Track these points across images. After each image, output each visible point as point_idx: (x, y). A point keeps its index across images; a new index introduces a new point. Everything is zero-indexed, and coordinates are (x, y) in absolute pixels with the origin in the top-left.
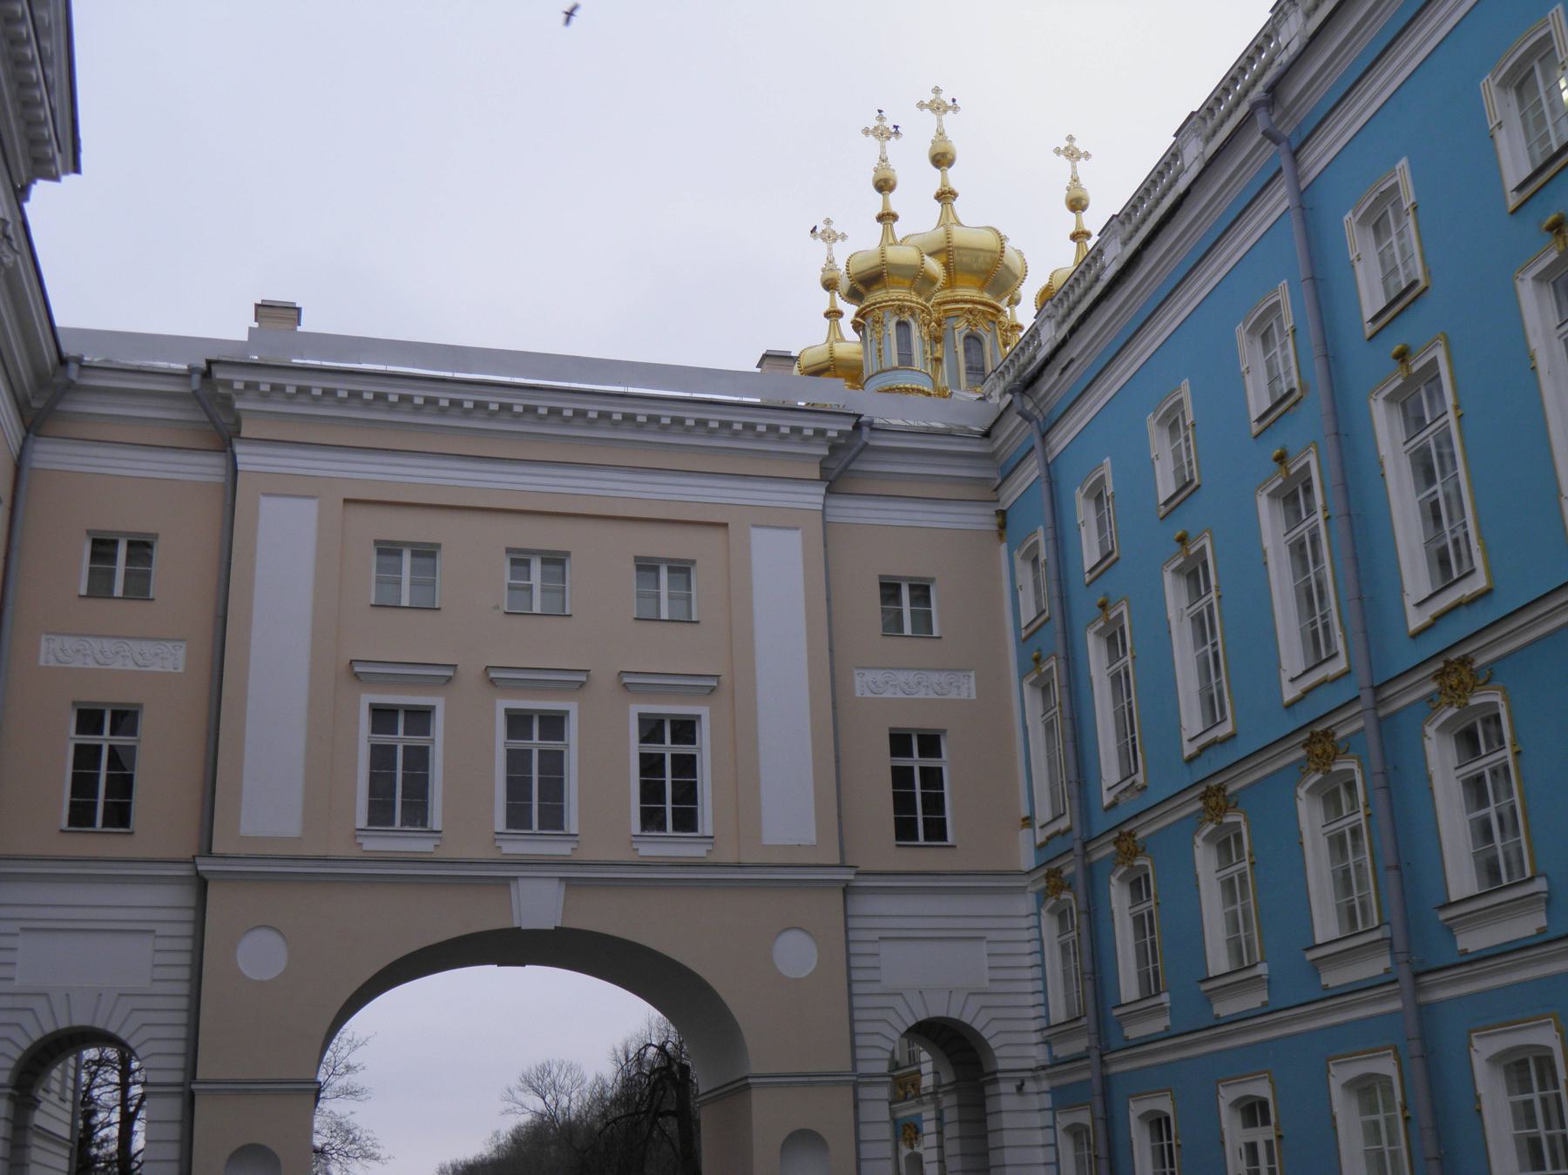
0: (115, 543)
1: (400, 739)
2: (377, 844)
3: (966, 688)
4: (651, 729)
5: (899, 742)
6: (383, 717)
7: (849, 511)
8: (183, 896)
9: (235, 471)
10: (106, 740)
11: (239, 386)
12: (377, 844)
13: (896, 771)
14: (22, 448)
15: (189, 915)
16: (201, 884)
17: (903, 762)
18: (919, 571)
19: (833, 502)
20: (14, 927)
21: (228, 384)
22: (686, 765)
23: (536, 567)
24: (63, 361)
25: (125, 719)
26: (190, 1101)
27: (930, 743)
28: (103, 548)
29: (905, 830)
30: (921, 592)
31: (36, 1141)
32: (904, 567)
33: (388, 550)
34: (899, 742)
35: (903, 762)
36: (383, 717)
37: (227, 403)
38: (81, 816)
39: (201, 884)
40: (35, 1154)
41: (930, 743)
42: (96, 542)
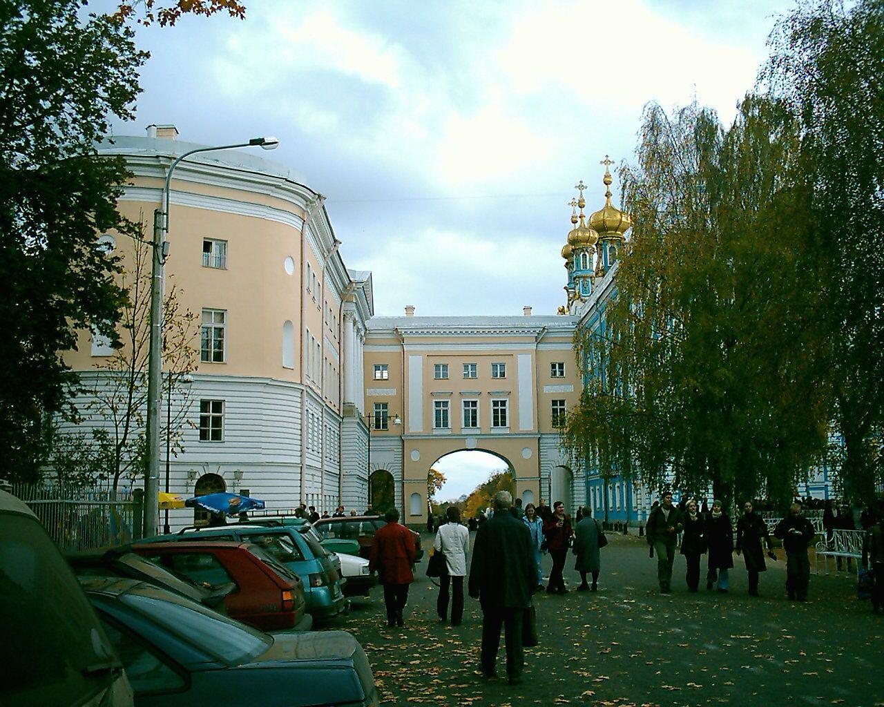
2: (435, 433)
3: (571, 389)
4: (495, 403)
5: (554, 403)
7: (542, 347)
13: (553, 409)
17: (555, 407)
18: (561, 362)
19: (539, 345)
22: (503, 411)
25: (385, 406)
26: (403, 484)
27: (562, 403)
29: (554, 423)
30: (561, 366)
32: (557, 361)
33: (437, 366)
34: (554, 403)
35: (555, 407)
36: (438, 404)
41: (562, 403)
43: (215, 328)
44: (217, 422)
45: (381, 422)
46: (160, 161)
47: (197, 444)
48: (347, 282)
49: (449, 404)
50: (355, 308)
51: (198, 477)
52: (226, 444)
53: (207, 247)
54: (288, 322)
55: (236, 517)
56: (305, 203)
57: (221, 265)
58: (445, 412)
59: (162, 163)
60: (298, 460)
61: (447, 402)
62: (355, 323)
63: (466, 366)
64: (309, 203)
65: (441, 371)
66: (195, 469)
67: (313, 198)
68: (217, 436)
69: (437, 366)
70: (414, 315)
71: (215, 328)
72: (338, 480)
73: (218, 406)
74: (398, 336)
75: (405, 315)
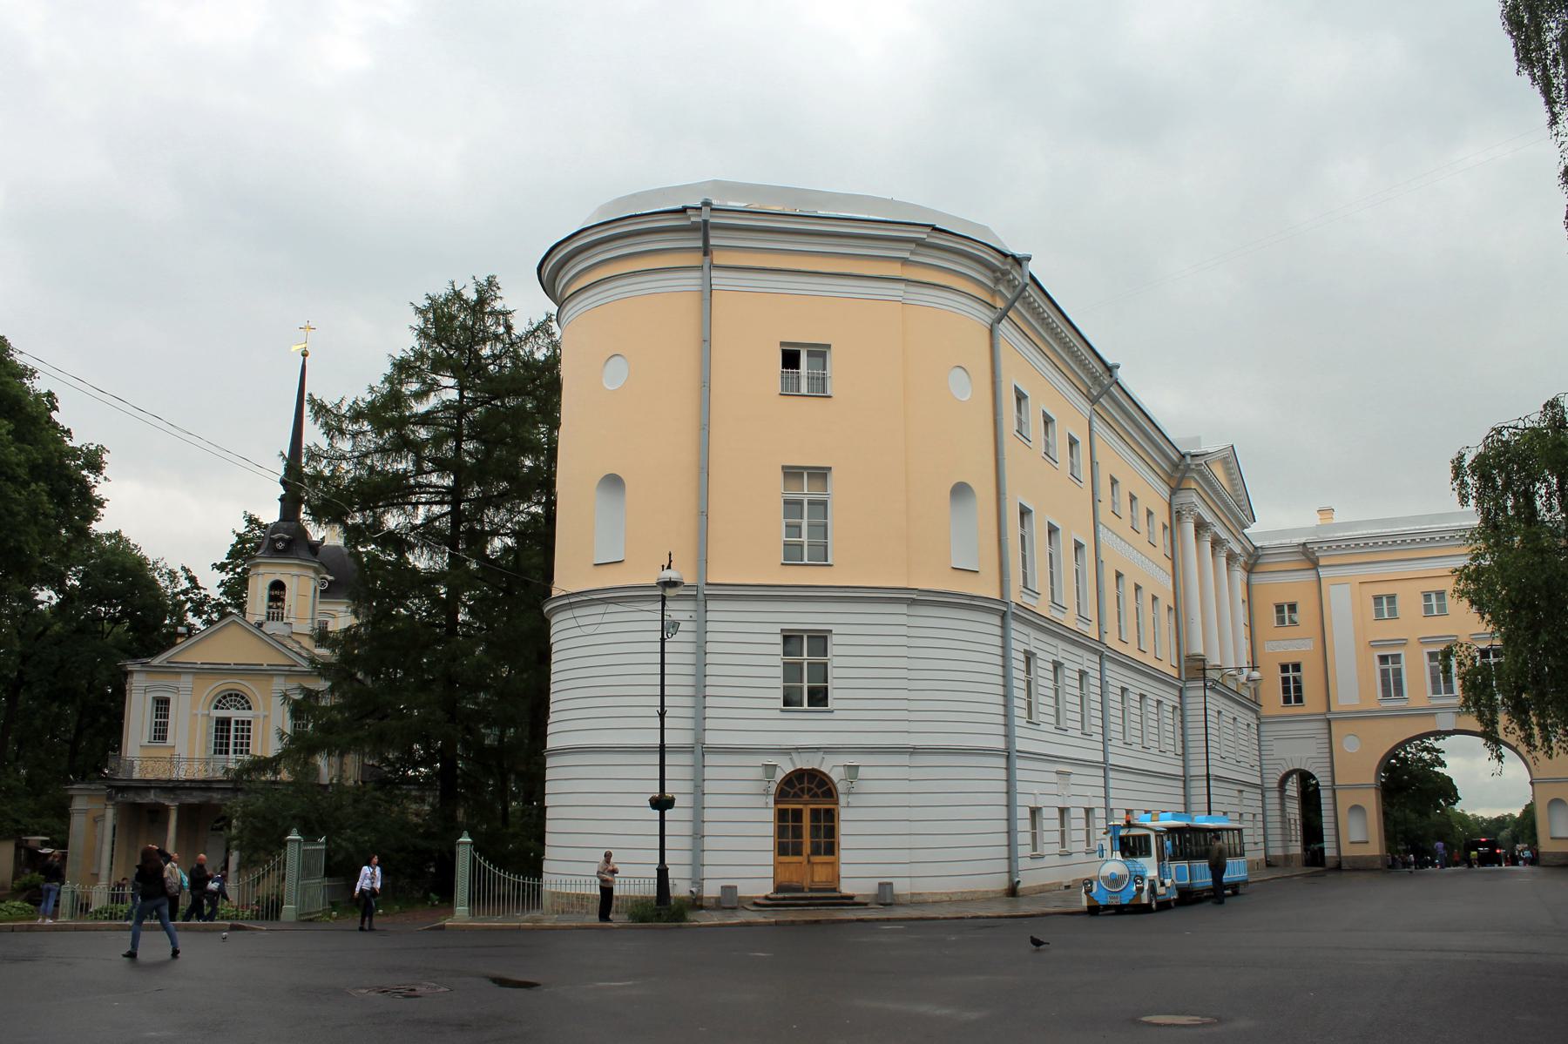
0: (1283, 606)
1: (1390, 666)
2: (1385, 704)
6: (1383, 659)
8: (1324, 725)
9: (1320, 579)
10: (1291, 674)
11: (1316, 549)
12: (1385, 704)
14: (1248, 579)
15: (1326, 731)
16: (1329, 721)
20: (1271, 738)
21: (1312, 548)
23: (1433, 597)
24: (1256, 548)
25: (1297, 667)
28: (1280, 608)
31: (1287, 800)
36: (1383, 659)
37: (1313, 553)
38: (1287, 700)
39: (1329, 721)
40: (1288, 804)
42: (1277, 607)
43: (810, 503)
44: (821, 671)
45: (1293, 692)
46: (689, 218)
47: (778, 714)
48: (1175, 457)
49: (1403, 657)
50: (1195, 499)
51: (780, 776)
52: (837, 715)
53: (790, 359)
54: (961, 491)
55: (322, 844)
56: (989, 274)
57: (819, 388)
58: (1398, 672)
59: (693, 219)
60: (1000, 743)
61: (1399, 655)
62: (1201, 526)
63: (1427, 596)
64: (999, 274)
65: (1385, 604)
66: (772, 760)
67: (1004, 264)
68: (819, 697)
69: (1378, 599)
70: (1334, 522)
71: (810, 503)
72: (1181, 791)
73: (820, 640)
74: (1309, 556)
75: (1319, 523)
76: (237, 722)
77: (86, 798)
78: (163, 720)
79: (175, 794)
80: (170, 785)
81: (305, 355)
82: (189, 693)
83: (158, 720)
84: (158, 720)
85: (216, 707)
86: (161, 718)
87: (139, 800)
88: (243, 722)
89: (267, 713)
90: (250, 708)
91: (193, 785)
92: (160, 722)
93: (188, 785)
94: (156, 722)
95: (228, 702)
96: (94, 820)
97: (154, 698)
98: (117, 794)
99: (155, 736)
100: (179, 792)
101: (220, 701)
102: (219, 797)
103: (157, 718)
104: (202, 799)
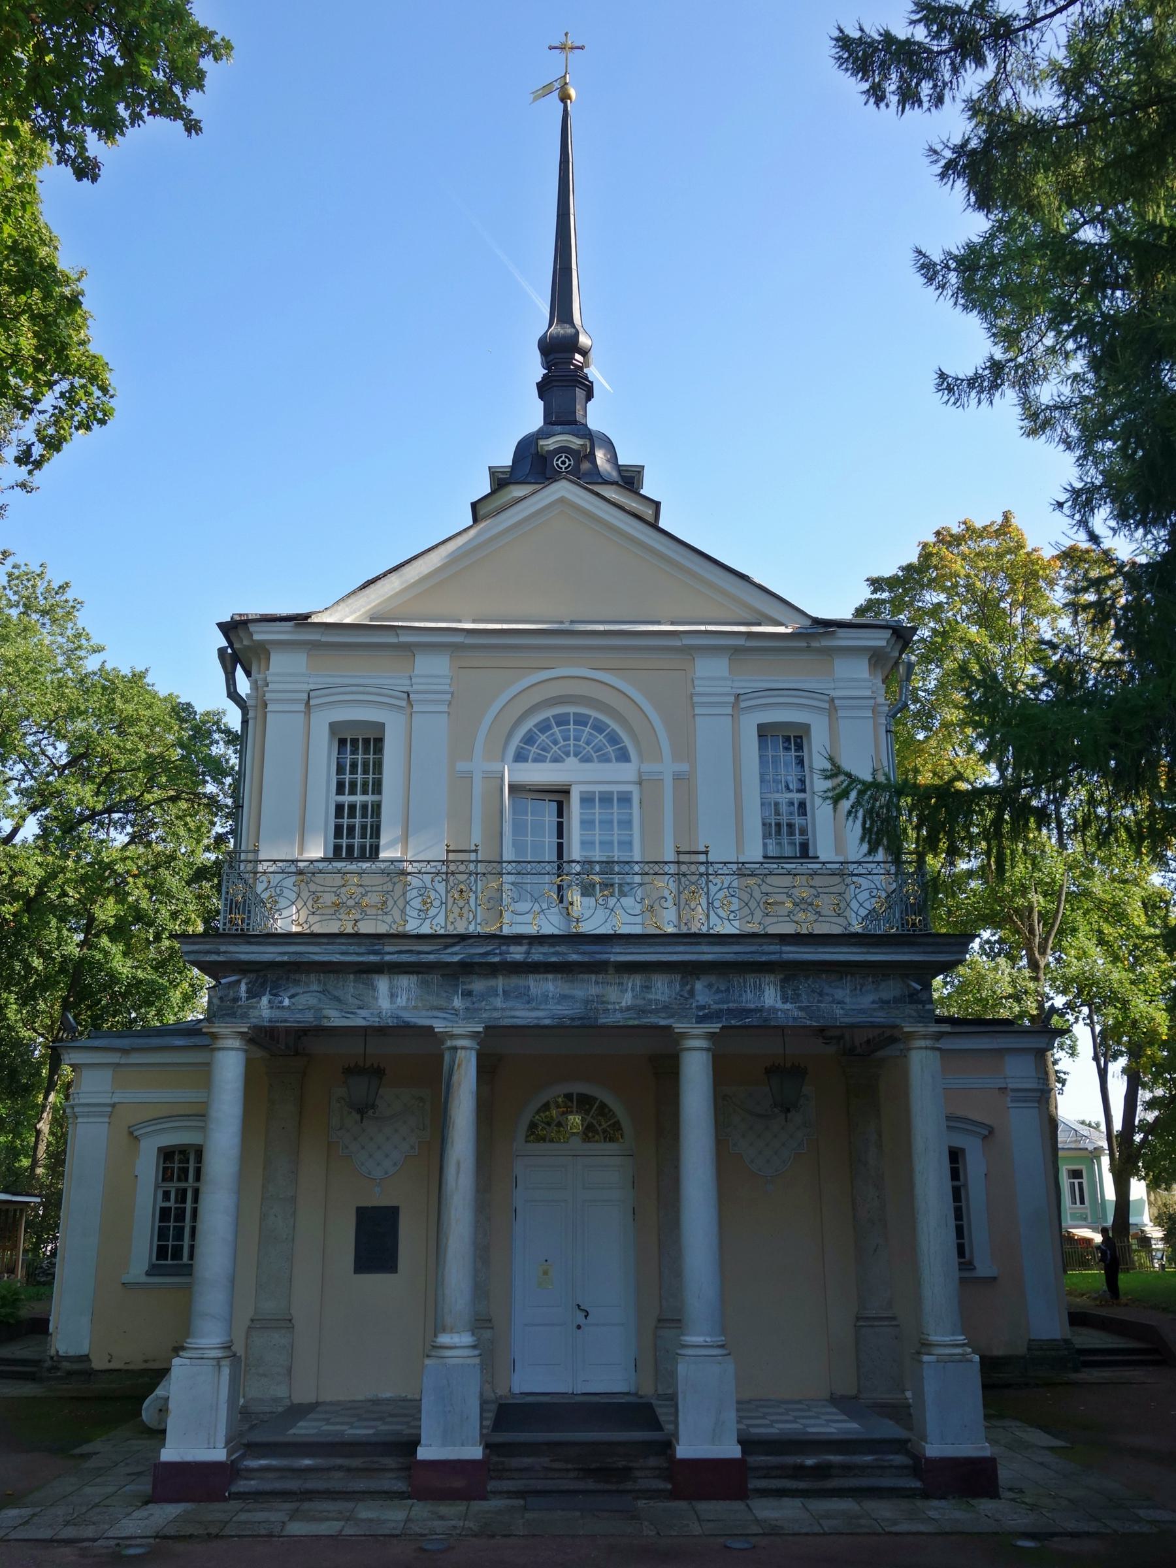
76: (587, 800)
77: (108, 1074)
78: (359, 799)
79: (468, 994)
80: (454, 955)
81: (564, 98)
82: (444, 708)
83: (347, 799)
84: (347, 799)
85: (520, 757)
86: (353, 792)
87: (335, 1018)
88: (606, 799)
89: (685, 767)
90: (624, 757)
91: (539, 954)
92: (352, 807)
93: (517, 953)
94: (339, 808)
95: (555, 743)
96: (131, 1133)
97: (334, 727)
98: (253, 994)
99: (337, 849)
100: (478, 985)
101: (529, 739)
102: (627, 999)
103: (340, 789)
104: (565, 1010)
